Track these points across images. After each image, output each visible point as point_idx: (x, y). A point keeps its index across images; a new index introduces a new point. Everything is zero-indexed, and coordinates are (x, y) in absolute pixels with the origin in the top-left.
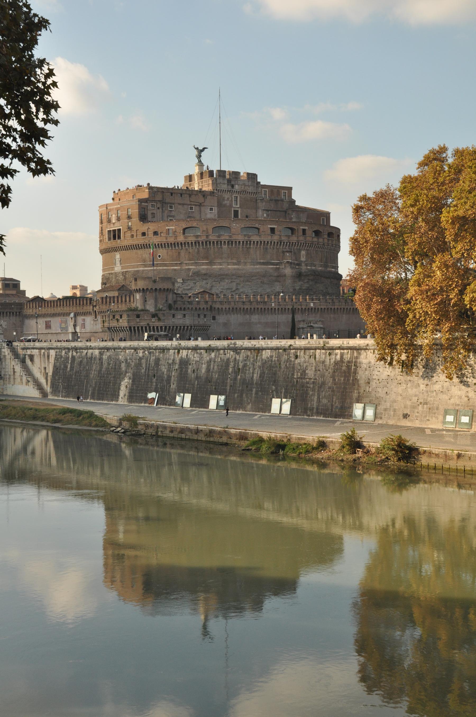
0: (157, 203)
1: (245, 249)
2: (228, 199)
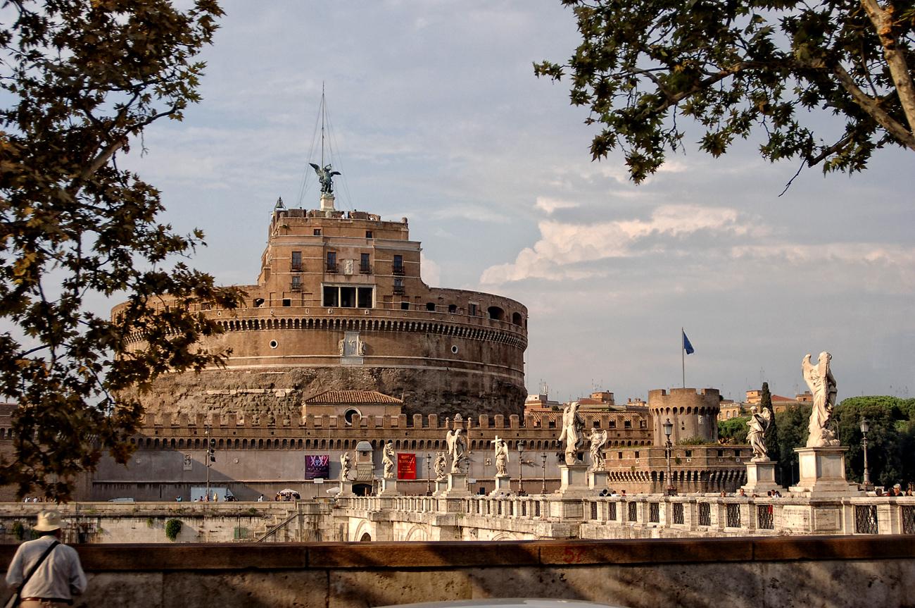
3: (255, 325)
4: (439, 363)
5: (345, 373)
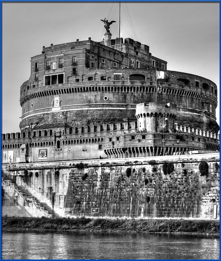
0: (95, 55)
1: (179, 97)
2: (134, 62)
4: (96, 106)
5: (53, 115)
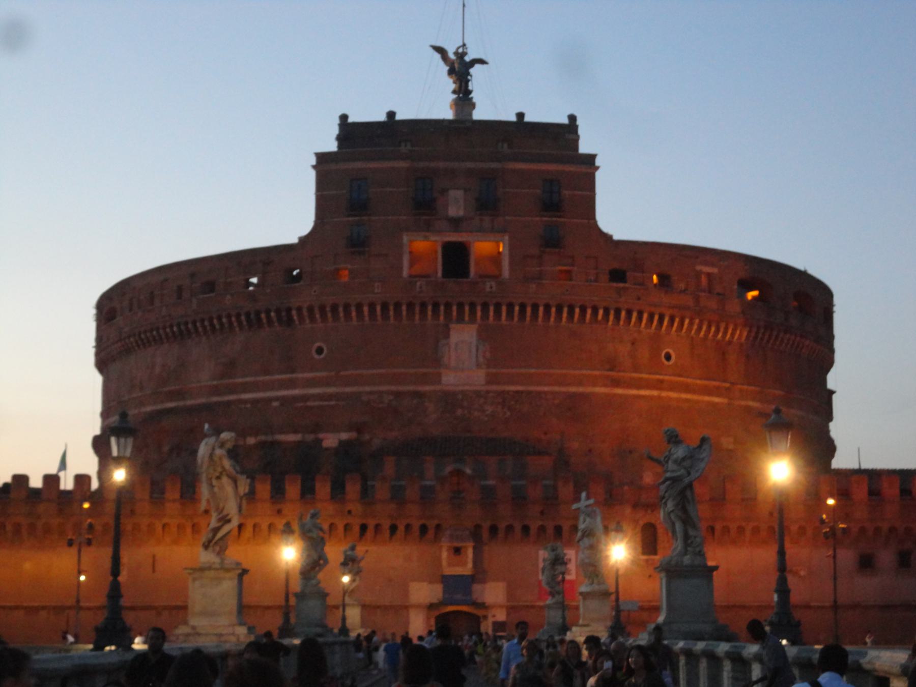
3: (286, 318)
5: (450, 400)
